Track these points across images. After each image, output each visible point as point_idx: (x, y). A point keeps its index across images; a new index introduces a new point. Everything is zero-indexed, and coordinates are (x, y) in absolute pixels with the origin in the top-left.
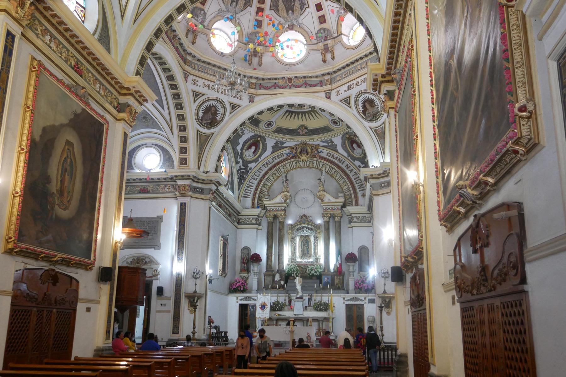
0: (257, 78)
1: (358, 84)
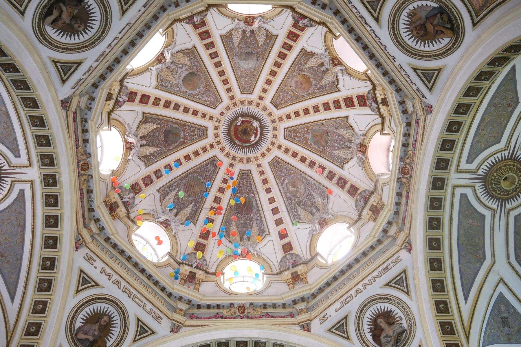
0: (189, 302)
1: (358, 292)
